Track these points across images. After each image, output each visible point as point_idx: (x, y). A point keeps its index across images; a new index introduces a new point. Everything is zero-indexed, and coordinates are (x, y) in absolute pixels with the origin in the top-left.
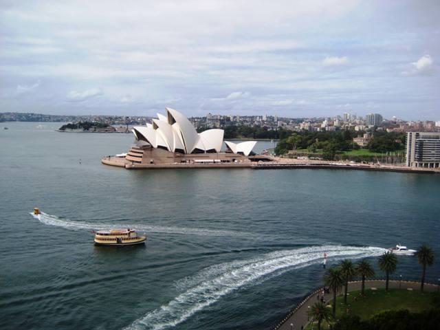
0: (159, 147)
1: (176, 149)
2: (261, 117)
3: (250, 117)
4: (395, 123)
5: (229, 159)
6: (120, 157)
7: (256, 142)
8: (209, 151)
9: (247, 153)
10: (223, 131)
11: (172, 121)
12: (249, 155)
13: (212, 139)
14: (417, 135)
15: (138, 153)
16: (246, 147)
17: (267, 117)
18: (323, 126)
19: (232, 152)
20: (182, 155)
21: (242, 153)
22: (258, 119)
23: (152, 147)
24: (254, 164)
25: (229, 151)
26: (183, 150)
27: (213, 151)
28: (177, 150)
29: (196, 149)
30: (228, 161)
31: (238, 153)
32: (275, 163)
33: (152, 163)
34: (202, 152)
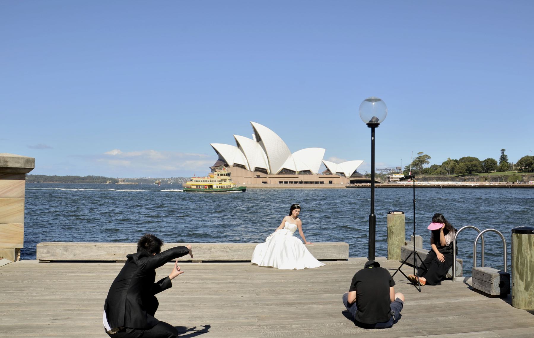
0: (236, 165)
8: (300, 173)
9: (348, 173)
10: (324, 150)
25: (328, 171)
26: (266, 169)
28: (257, 169)
29: (284, 169)
30: (322, 183)
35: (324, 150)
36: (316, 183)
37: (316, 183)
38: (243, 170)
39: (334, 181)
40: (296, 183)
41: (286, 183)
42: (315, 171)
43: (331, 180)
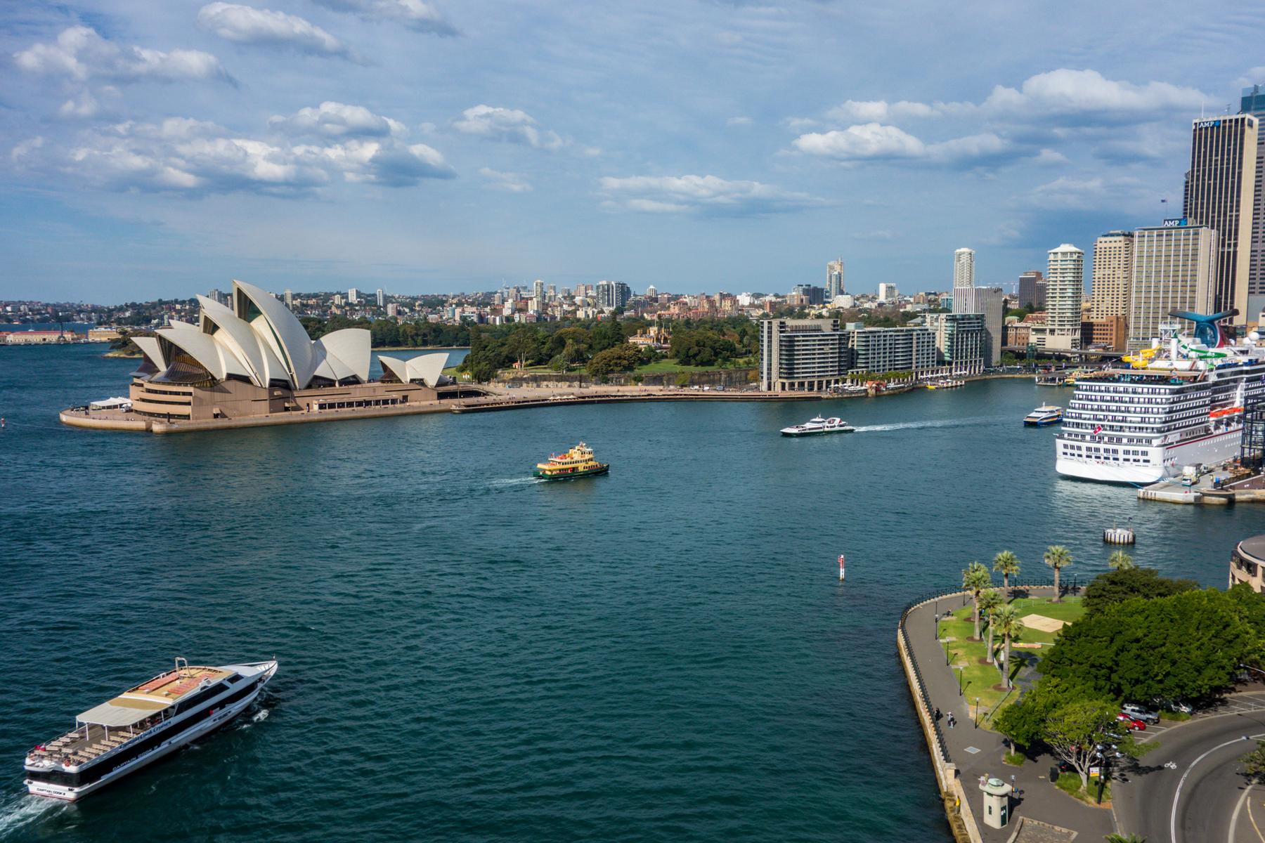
0: (230, 377)
1: (271, 380)
2: (345, 296)
3: (316, 296)
4: (656, 300)
5: (394, 395)
6: (109, 407)
7: (446, 355)
8: (344, 382)
9: (432, 381)
10: (369, 332)
11: (248, 310)
12: (438, 385)
13: (346, 352)
14: (782, 325)
15: (177, 393)
16: (428, 366)
17: (359, 295)
18: (507, 312)
20: (287, 393)
21: (421, 382)
22: (337, 300)
23: (213, 378)
24: (453, 404)
25: (389, 376)
27: (353, 381)
28: (275, 383)
31: (412, 381)
32: (498, 399)
33: (216, 416)
34: (330, 383)
35: (369, 332)
36: (385, 402)
38: (249, 386)
39: (411, 395)
40: (350, 404)
41: (332, 406)
42: (364, 376)
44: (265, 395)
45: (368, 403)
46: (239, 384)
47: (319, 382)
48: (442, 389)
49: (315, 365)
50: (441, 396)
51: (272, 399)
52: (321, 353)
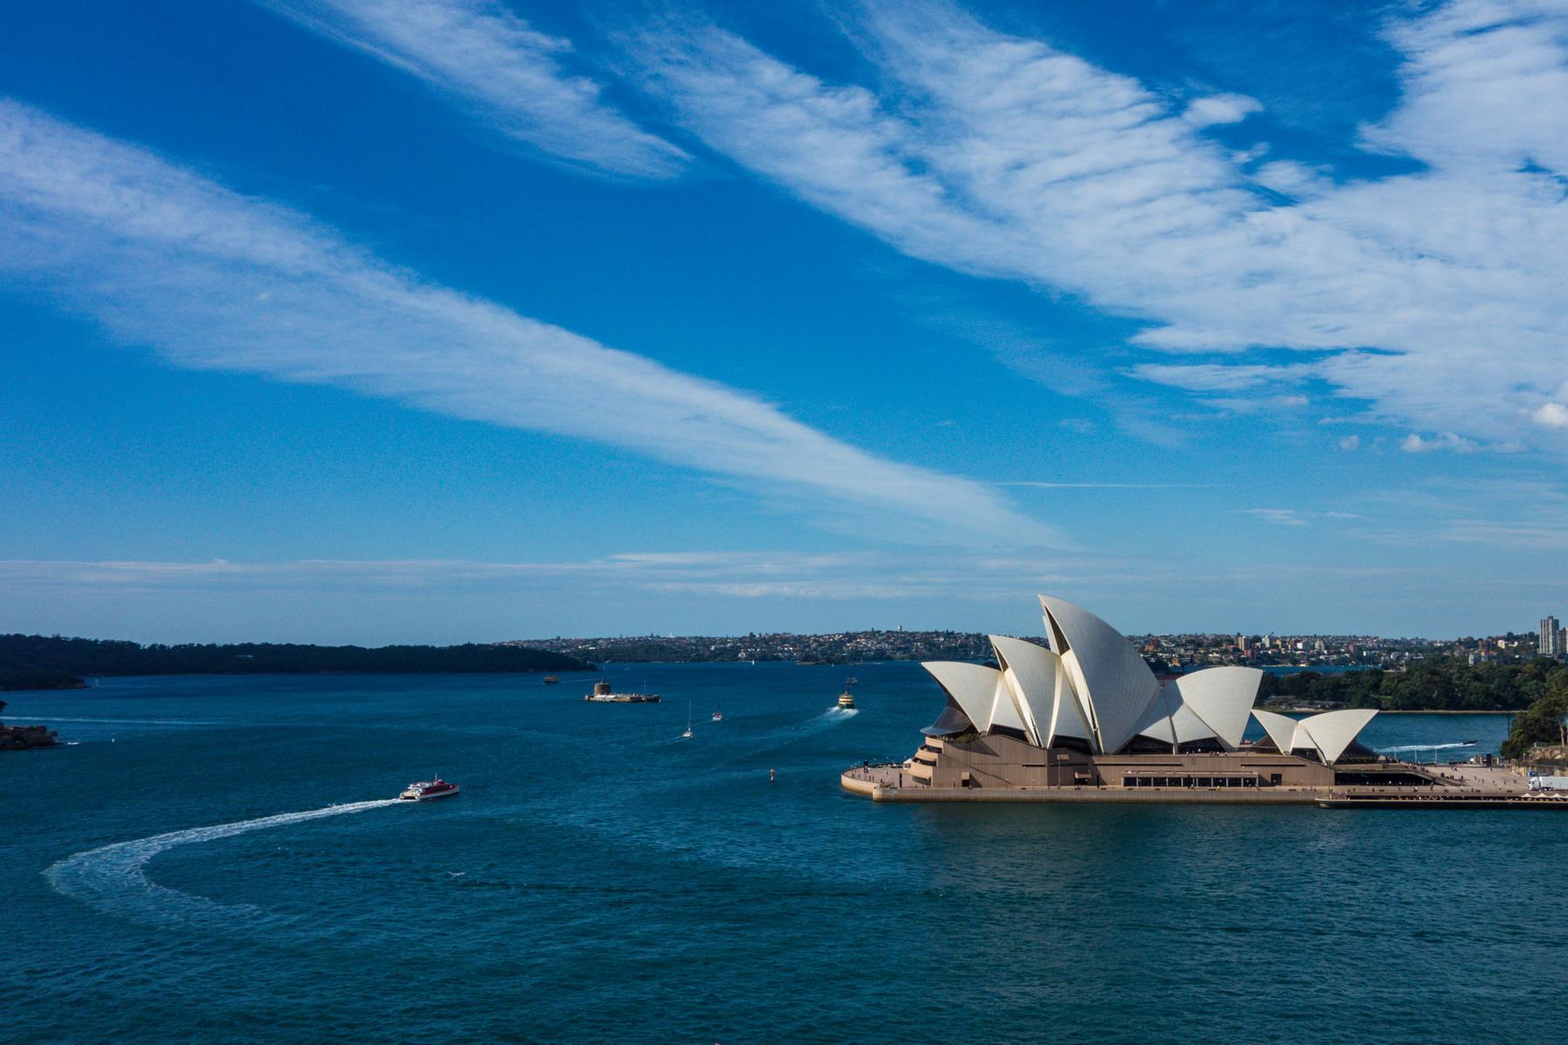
0: (997, 730)
1: (1056, 738)
12: (1339, 762)
16: (1331, 731)
19: (1277, 751)
20: (1079, 758)
25: (1268, 746)
26: (1085, 741)
28: (1060, 742)
31: (1296, 752)
36: (1235, 782)
37: (1235, 782)
38: (1020, 744)
39: (1287, 774)
40: (1175, 782)
41: (1145, 782)
43: (1276, 771)
44: (1042, 759)
45: (1219, 782)
46: (1006, 741)
47: (1139, 746)
48: (1344, 768)
49: (1150, 717)
50: (1341, 779)
51: (1053, 764)
52: (1172, 701)
